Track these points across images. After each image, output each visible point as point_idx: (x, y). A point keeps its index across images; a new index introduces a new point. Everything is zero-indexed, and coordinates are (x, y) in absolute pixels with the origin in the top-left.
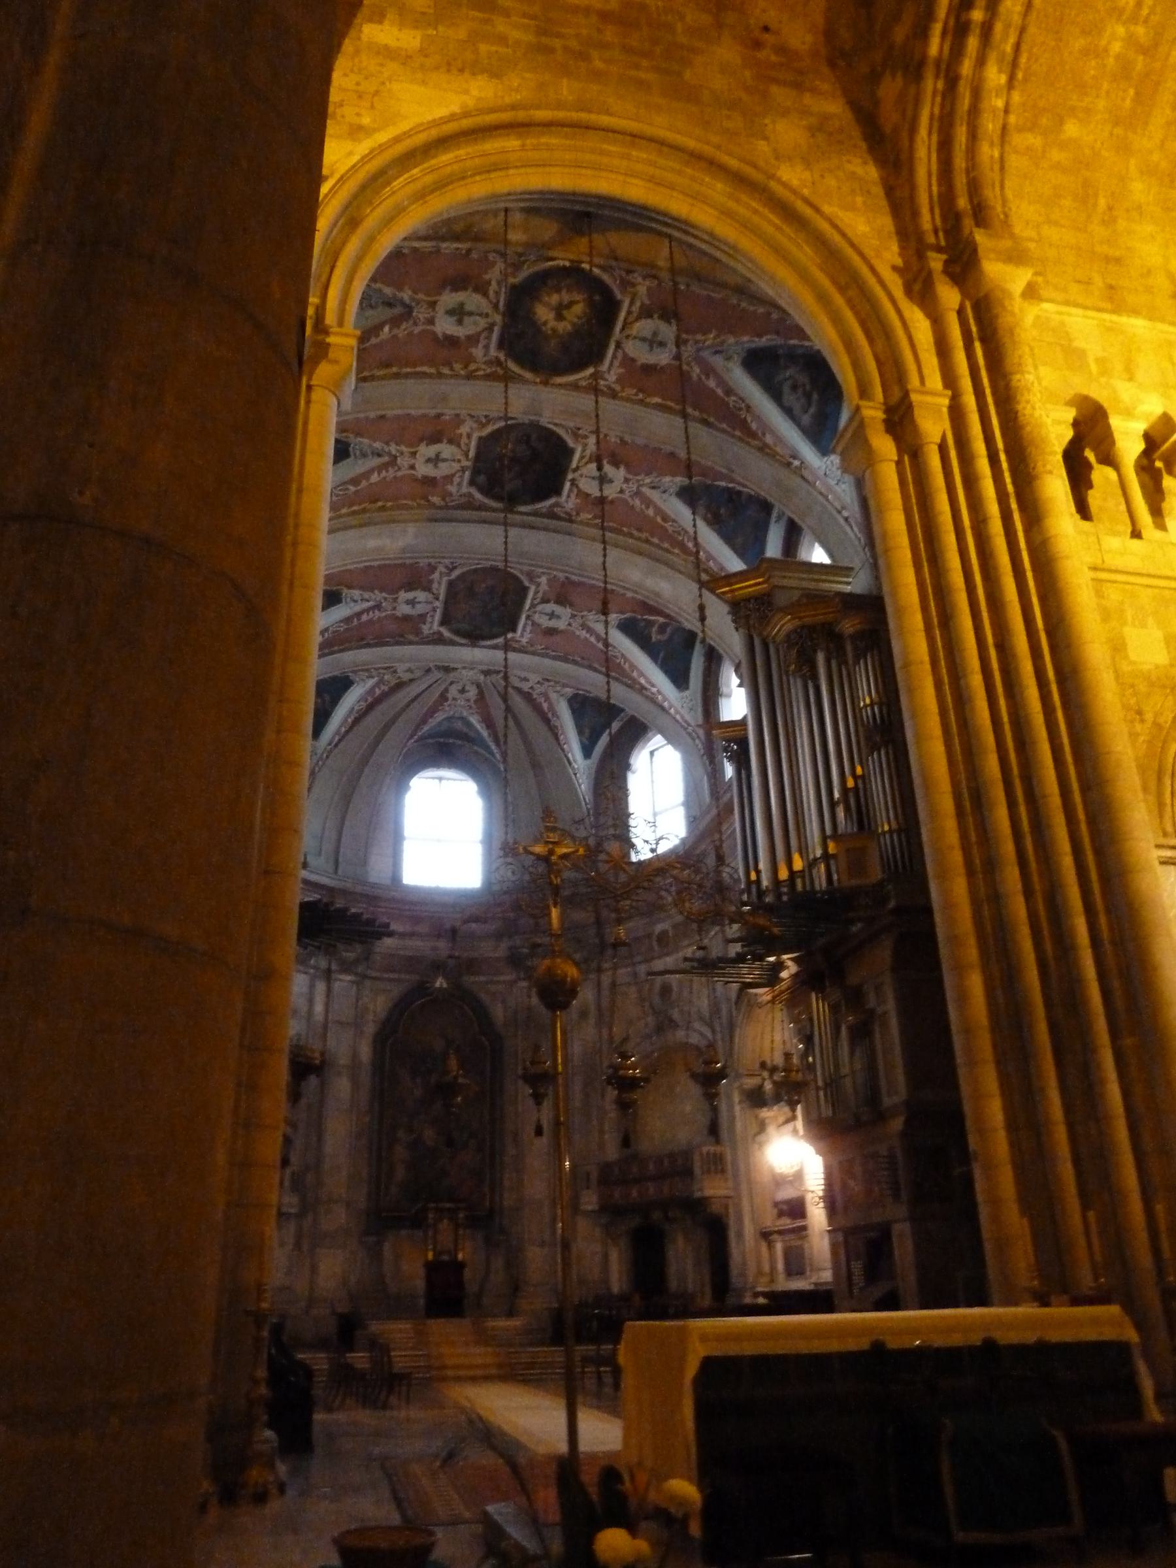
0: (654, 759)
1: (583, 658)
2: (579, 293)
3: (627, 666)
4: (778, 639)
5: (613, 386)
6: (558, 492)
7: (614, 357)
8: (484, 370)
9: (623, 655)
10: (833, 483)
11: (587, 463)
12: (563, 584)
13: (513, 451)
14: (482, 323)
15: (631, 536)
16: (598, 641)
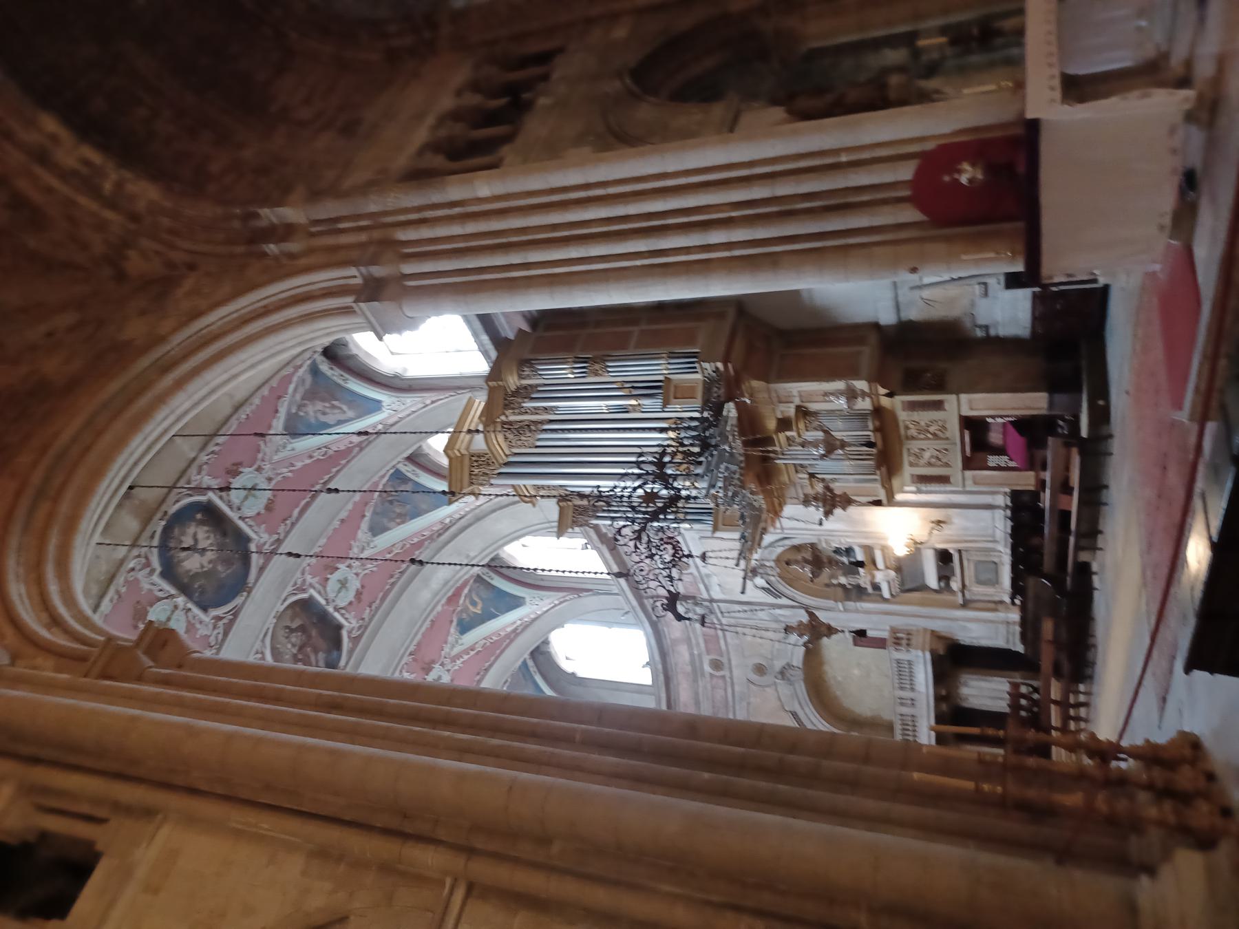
0: (571, 658)
1: (478, 674)
2: (189, 528)
3: (495, 638)
4: (508, 452)
5: (272, 540)
6: (339, 627)
7: (250, 526)
8: (219, 633)
9: (484, 639)
10: (403, 407)
11: (326, 592)
12: (414, 660)
13: (294, 645)
14: (179, 614)
15: (393, 584)
16: (468, 654)
